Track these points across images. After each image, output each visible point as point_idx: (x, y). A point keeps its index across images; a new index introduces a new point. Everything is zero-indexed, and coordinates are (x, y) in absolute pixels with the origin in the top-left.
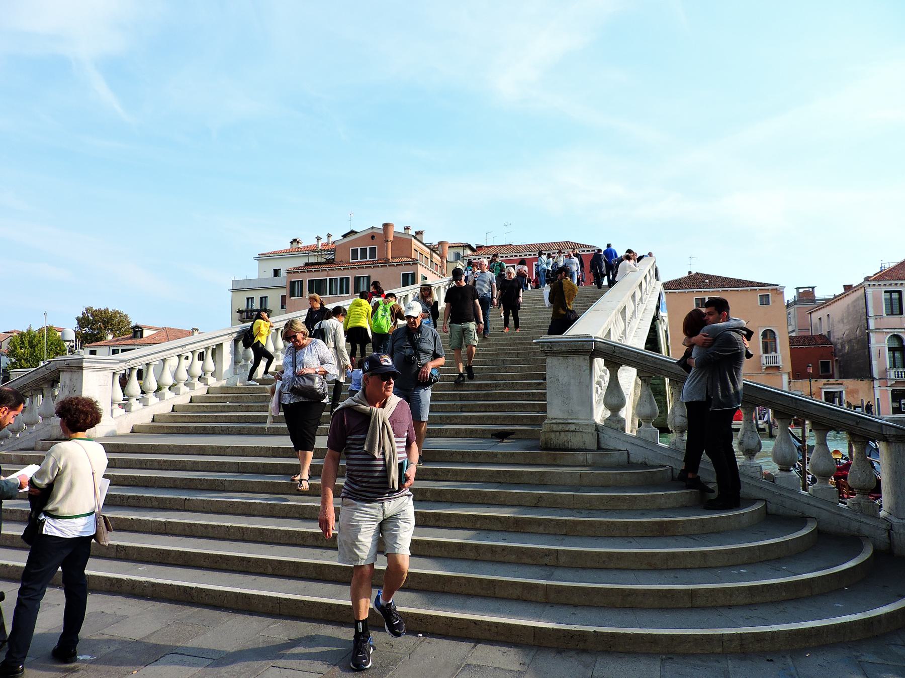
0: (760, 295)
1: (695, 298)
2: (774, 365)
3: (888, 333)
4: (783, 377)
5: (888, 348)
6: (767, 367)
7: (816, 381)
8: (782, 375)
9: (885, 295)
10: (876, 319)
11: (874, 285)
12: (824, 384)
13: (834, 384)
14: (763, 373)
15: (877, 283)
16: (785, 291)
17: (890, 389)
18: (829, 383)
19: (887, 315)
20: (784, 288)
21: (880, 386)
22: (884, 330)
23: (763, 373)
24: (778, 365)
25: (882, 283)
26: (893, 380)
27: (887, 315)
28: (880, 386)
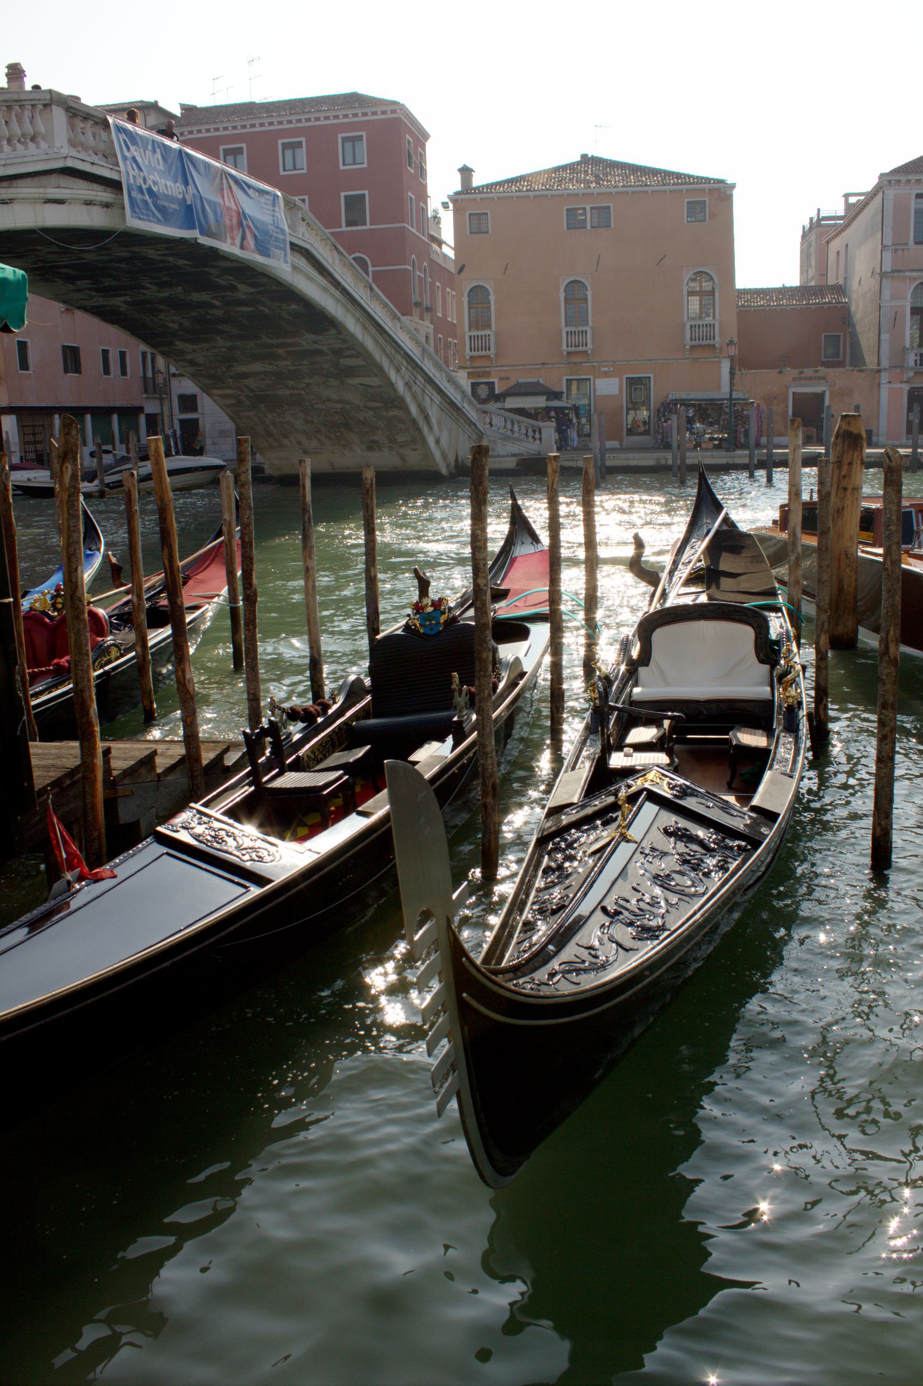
0: (688, 203)
1: (565, 209)
2: (705, 342)
3: (915, 279)
4: (722, 365)
5: (912, 308)
6: (691, 346)
7: (780, 372)
8: (720, 363)
9: (916, 203)
10: (896, 250)
11: (898, 181)
12: (794, 379)
13: (810, 378)
14: (687, 358)
15: (903, 178)
16: (736, 193)
17: (906, 387)
18: (802, 376)
19: (916, 243)
20: (733, 186)
21: (889, 382)
22: (908, 274)
23: (687, 358)
24: (712, 342)
25: (913, 177)
26: (911, 369)
27: (916, 243)
28: (889, 382)
